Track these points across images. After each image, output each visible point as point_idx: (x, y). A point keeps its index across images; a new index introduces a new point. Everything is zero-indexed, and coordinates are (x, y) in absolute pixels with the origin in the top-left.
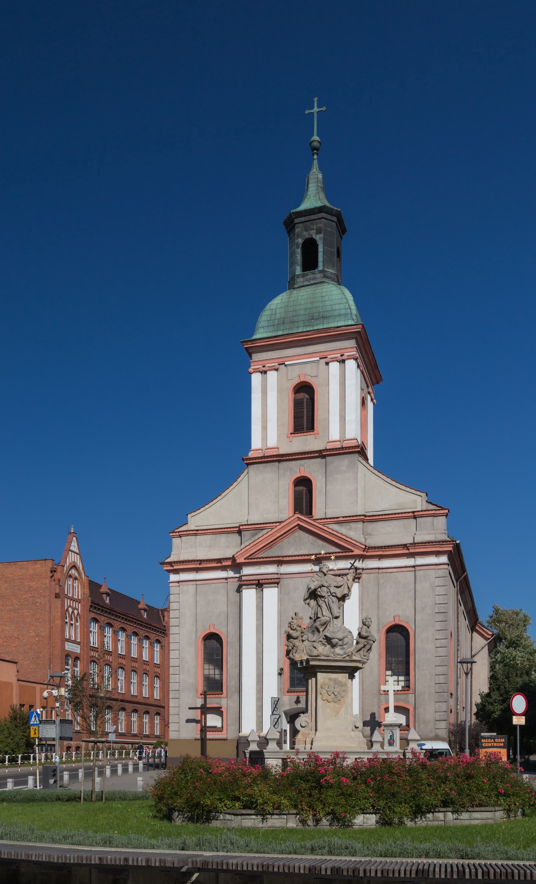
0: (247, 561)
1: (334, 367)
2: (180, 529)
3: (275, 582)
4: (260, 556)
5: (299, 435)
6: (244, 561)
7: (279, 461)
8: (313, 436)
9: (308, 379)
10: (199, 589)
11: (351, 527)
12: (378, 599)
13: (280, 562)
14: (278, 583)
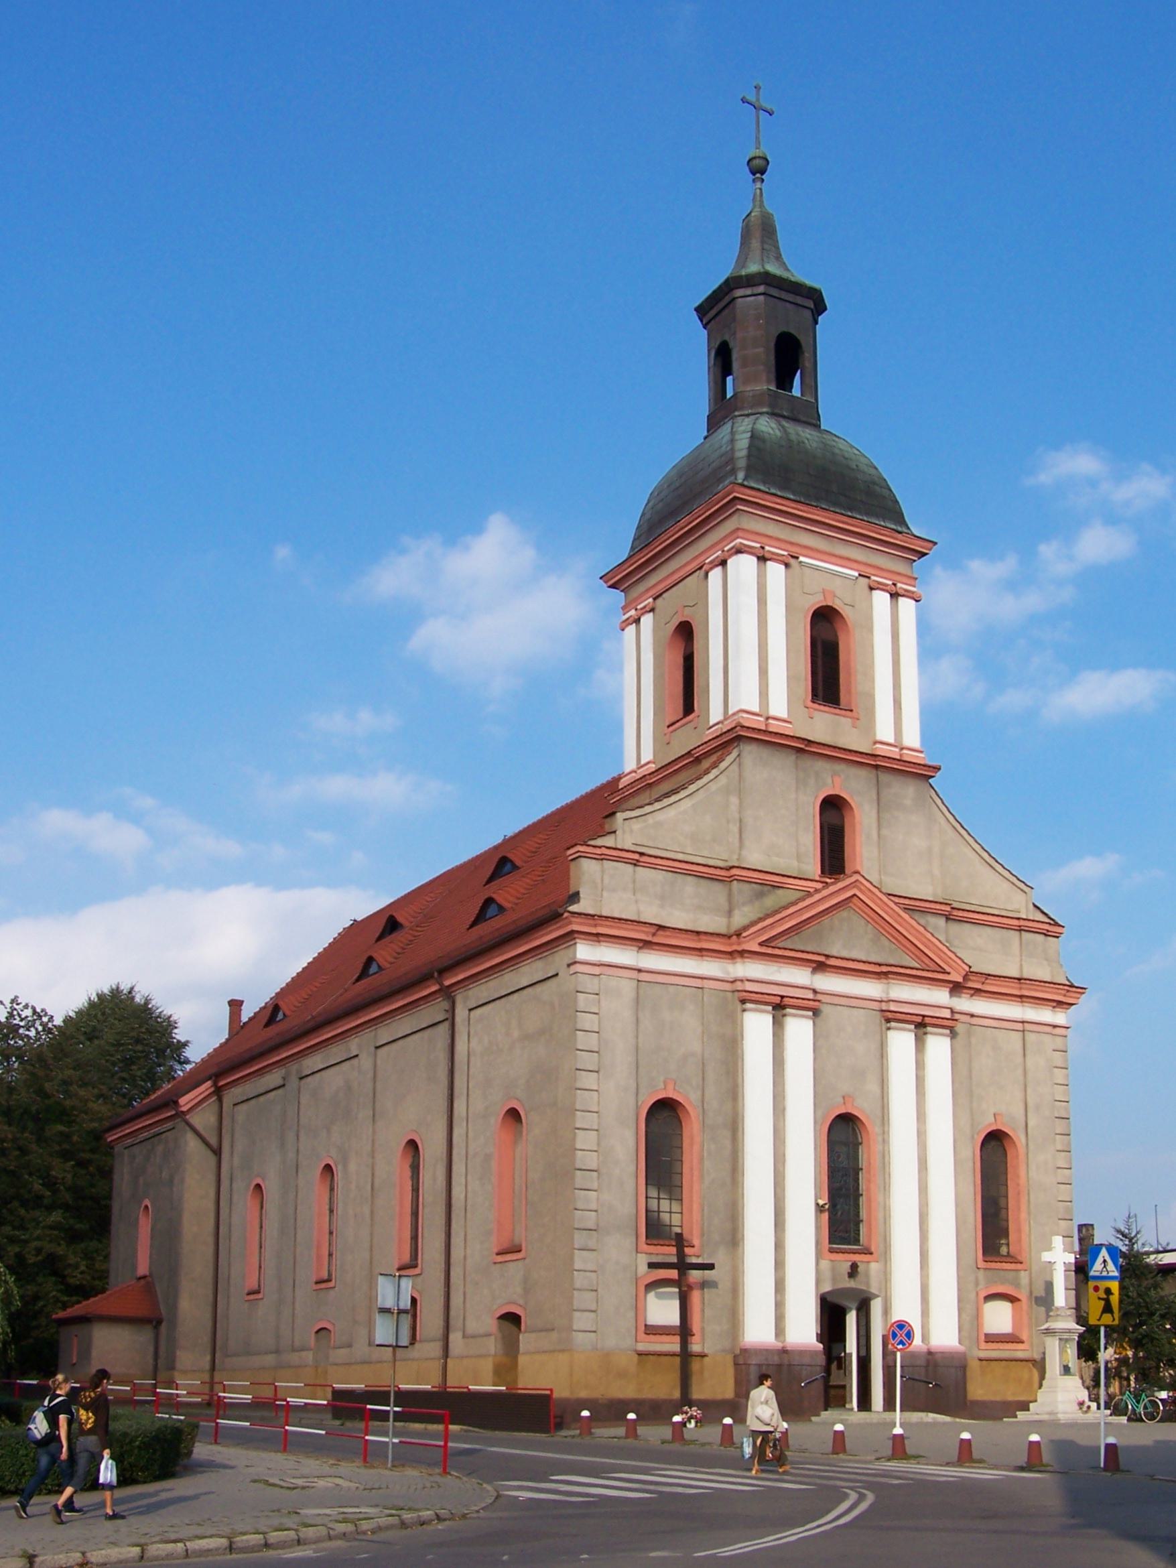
0: (764, 950)
1: (881, 599)
2: (599, 842)
3: (813, 1006)
4: (780, 945)
5: (826, 709)
6: (757, 949)
7: (800, 751)
8: (849, 720)
9: (837, 605)
10: (641, 992)
11: (927, 921)
12: (971, 1078)
13: (820, 967)
14: (816, 1012)
